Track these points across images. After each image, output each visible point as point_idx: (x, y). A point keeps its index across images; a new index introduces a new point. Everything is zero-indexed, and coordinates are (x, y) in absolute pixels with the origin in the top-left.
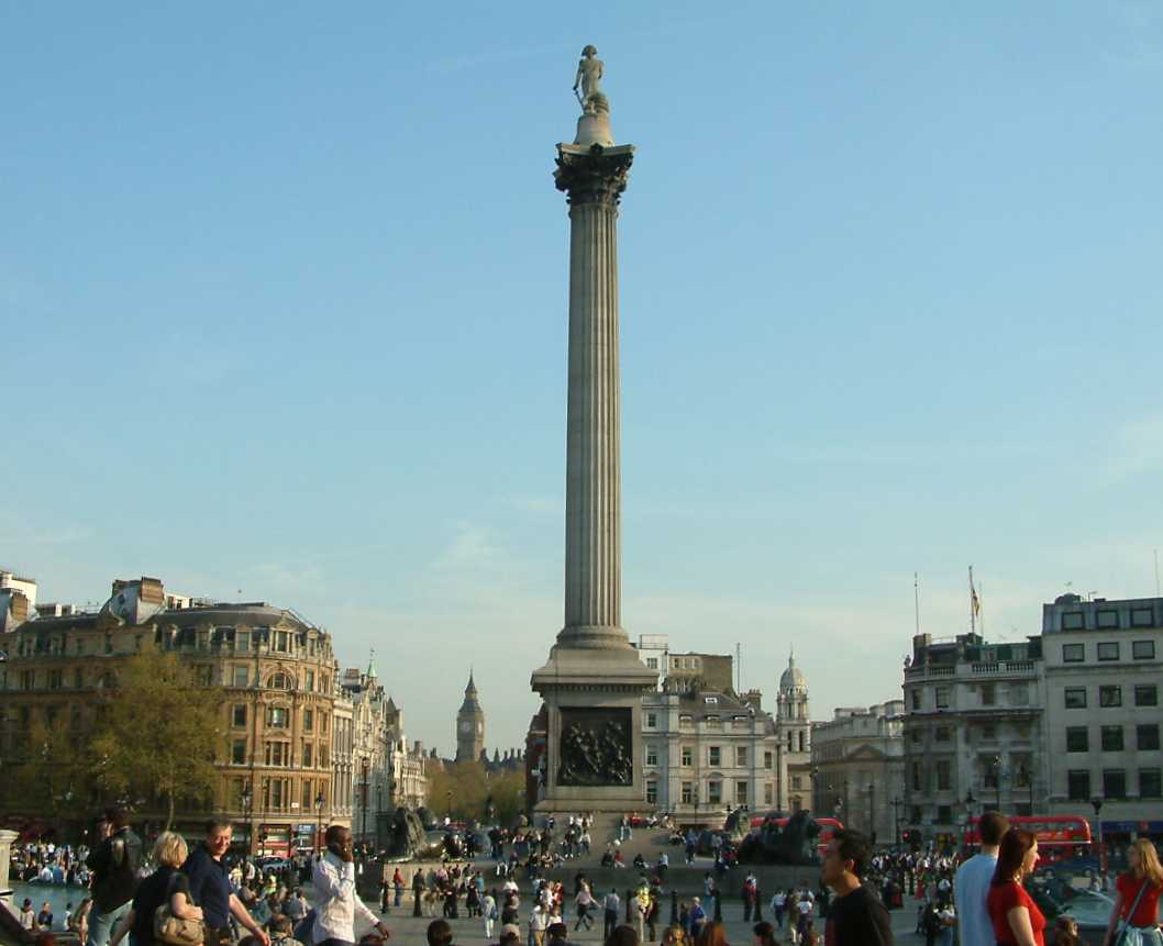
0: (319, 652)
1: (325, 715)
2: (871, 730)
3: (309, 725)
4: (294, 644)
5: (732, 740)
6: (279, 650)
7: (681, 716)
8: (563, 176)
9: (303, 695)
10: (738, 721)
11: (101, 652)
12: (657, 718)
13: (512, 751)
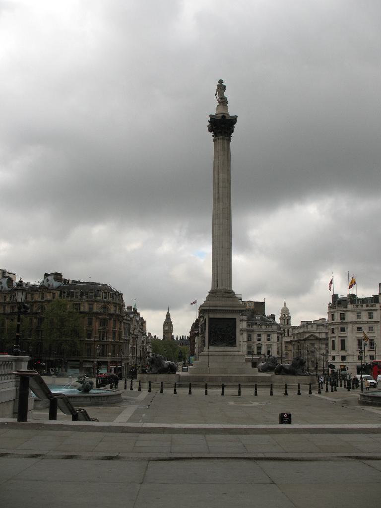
1: (121, 322)
8: (212, 126)
11: (39, 299)
13: (185, 337)
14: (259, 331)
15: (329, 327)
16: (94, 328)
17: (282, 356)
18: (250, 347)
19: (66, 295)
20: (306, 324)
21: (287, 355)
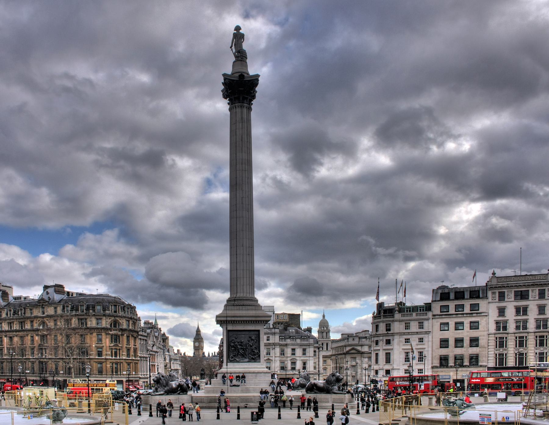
0: (131, 313)
2: (356, 341)
3: (128, 341)
4: (120, 310)
5: (301, 345)
6: (114, 312)
7: (279, 337)
9: (125, 330)
10: (303, 339)
12: (270, 337)
13: (215, 353)
14: (293, 345)
15: (373, 339)
16: (104, 345)
17: (319, 371)
18: (284, 362)
19: (69, 309)
20: (347, 337)
21: (326, 369)
